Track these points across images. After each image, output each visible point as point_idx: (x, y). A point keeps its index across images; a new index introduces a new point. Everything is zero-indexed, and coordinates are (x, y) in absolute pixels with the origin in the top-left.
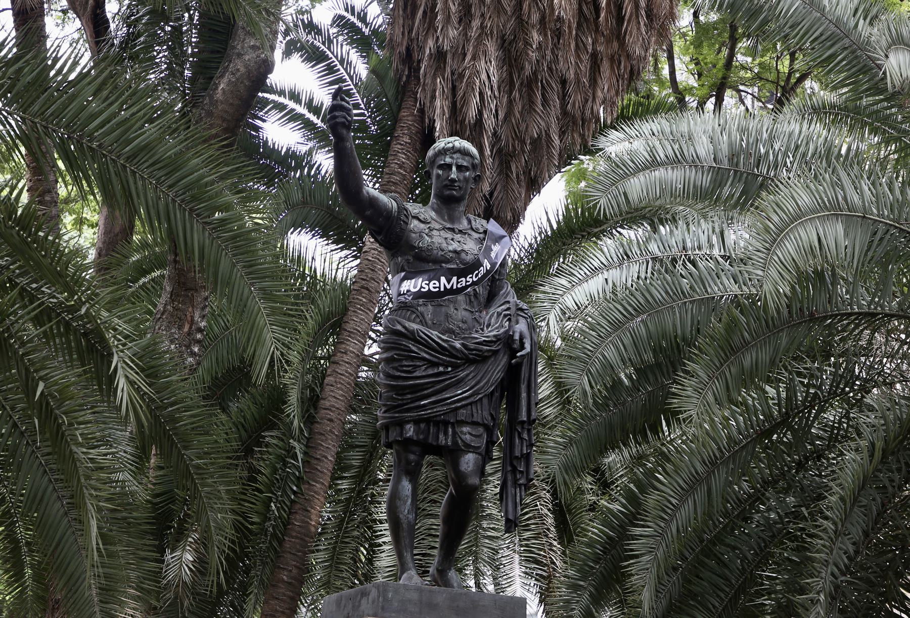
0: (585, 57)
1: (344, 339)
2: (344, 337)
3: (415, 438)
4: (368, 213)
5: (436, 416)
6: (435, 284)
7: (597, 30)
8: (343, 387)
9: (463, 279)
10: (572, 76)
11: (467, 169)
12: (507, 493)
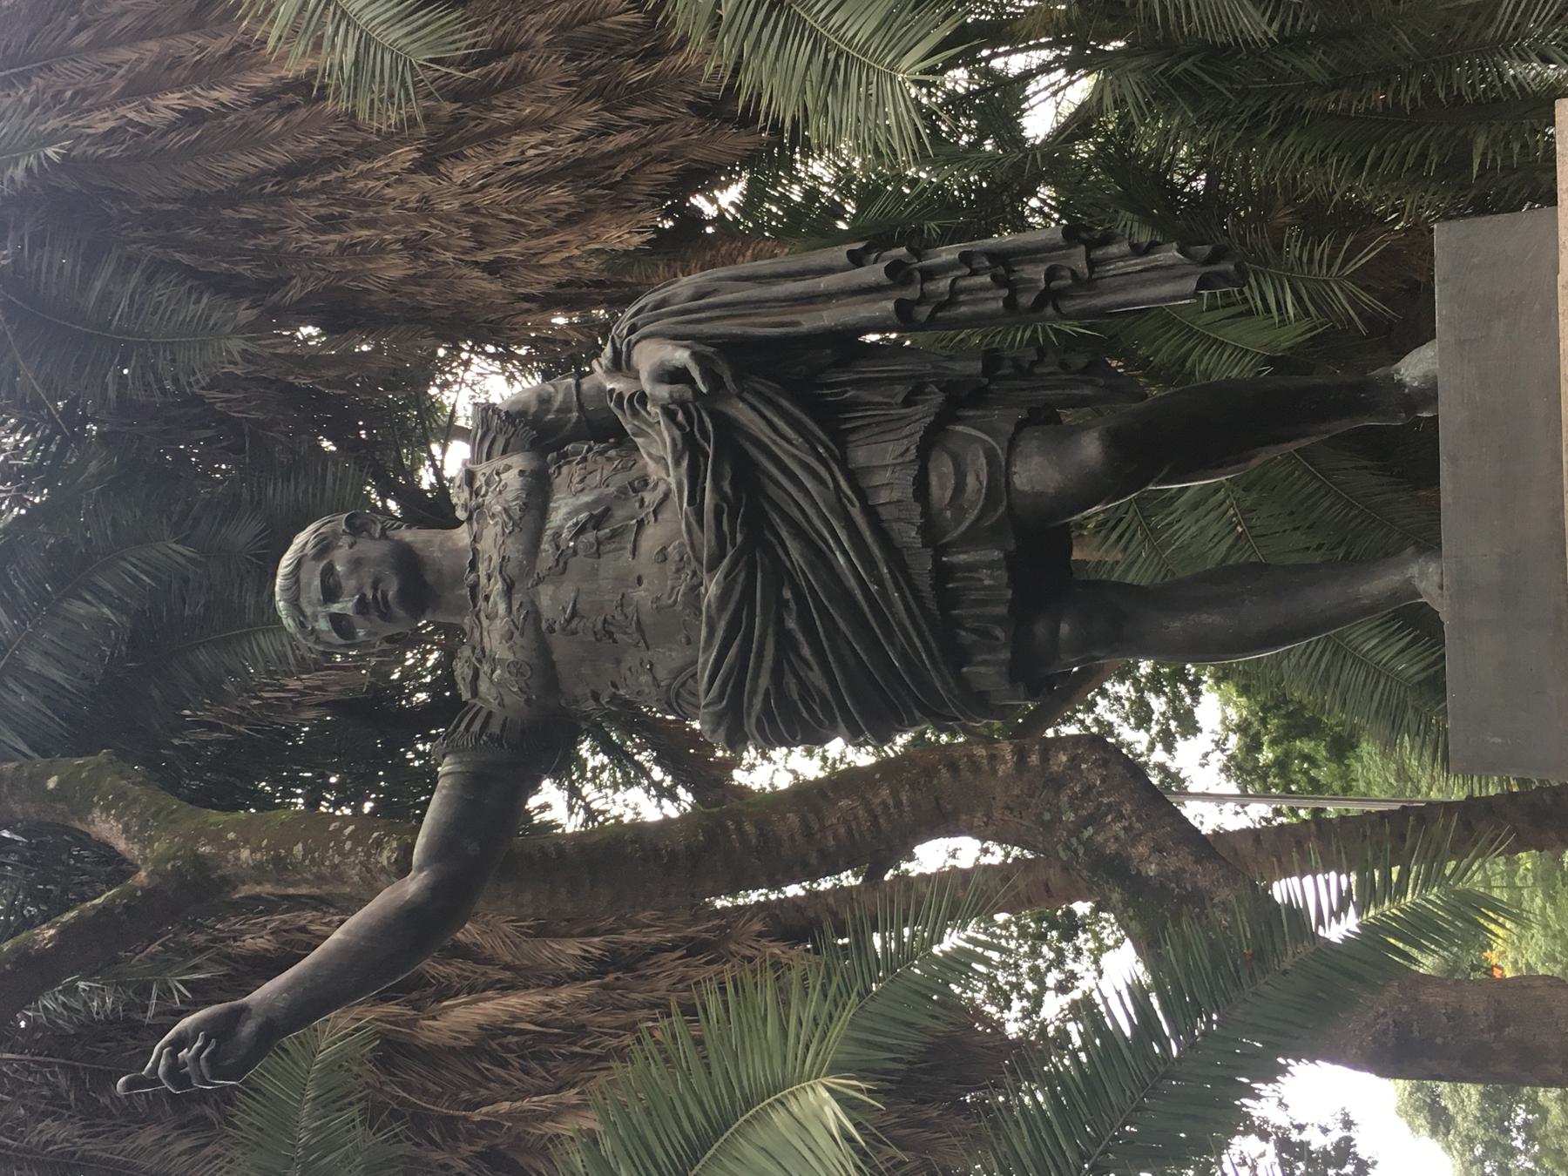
3: (1005, 655)
11: (329, 570)
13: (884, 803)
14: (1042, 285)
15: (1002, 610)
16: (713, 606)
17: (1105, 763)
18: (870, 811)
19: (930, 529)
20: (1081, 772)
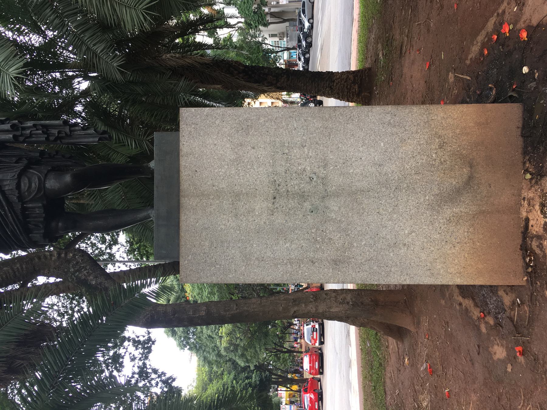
3: (42, 231)
13: (18, 268)
14: (57, 135)
15: (42, 219)
17: (83, 256)
18: (13, 271)
19: (21, 198)
20: (76, 258)
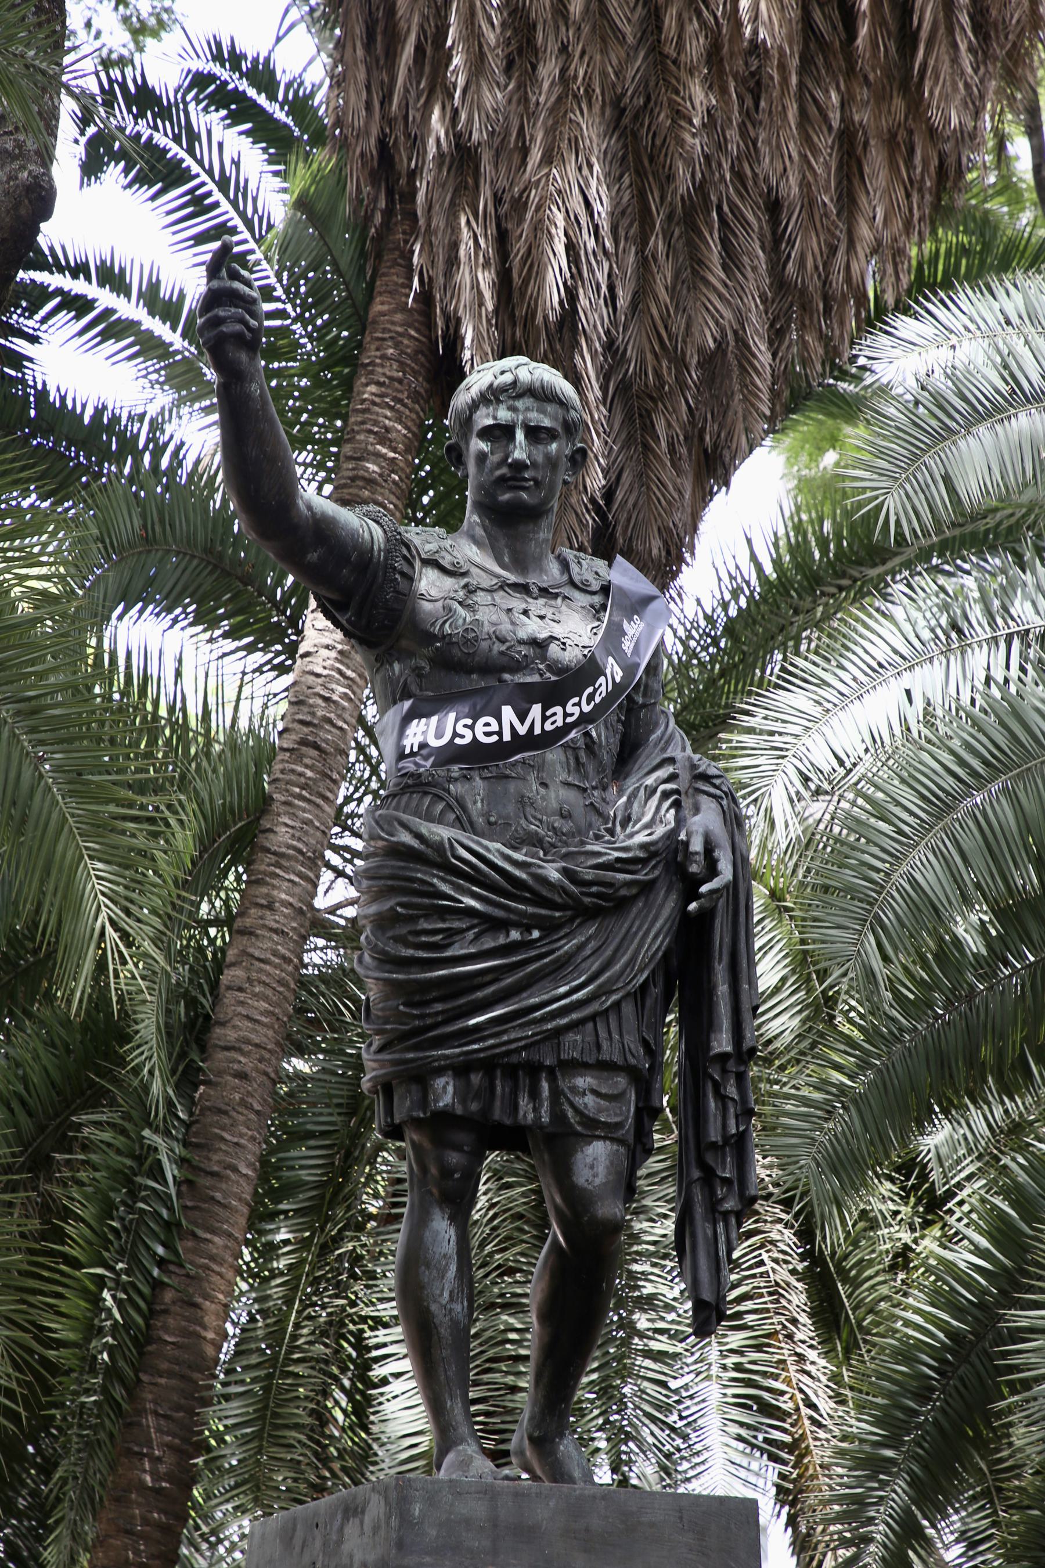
0: (825, 141)
1: (264, 873)
2: (263, 867)
3: (459, 1110)
4: (313, 557)
5: (508, 1053)
6: (487, 724)
7: (851, 71)
8: (269, 992)
9: (558, 709)
10: (795, 190)
11: (552, 434)
12: (693, 1236)
16: (540, 871)
